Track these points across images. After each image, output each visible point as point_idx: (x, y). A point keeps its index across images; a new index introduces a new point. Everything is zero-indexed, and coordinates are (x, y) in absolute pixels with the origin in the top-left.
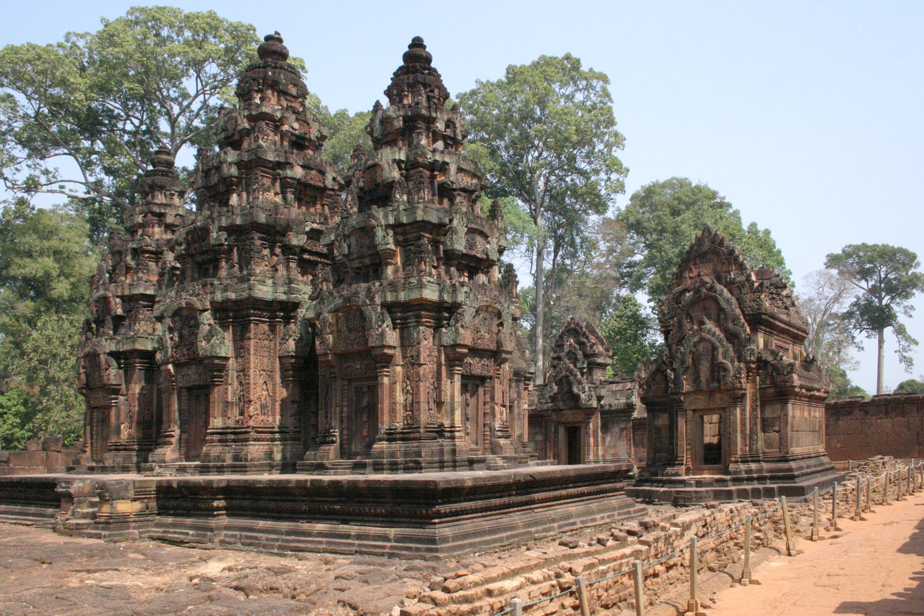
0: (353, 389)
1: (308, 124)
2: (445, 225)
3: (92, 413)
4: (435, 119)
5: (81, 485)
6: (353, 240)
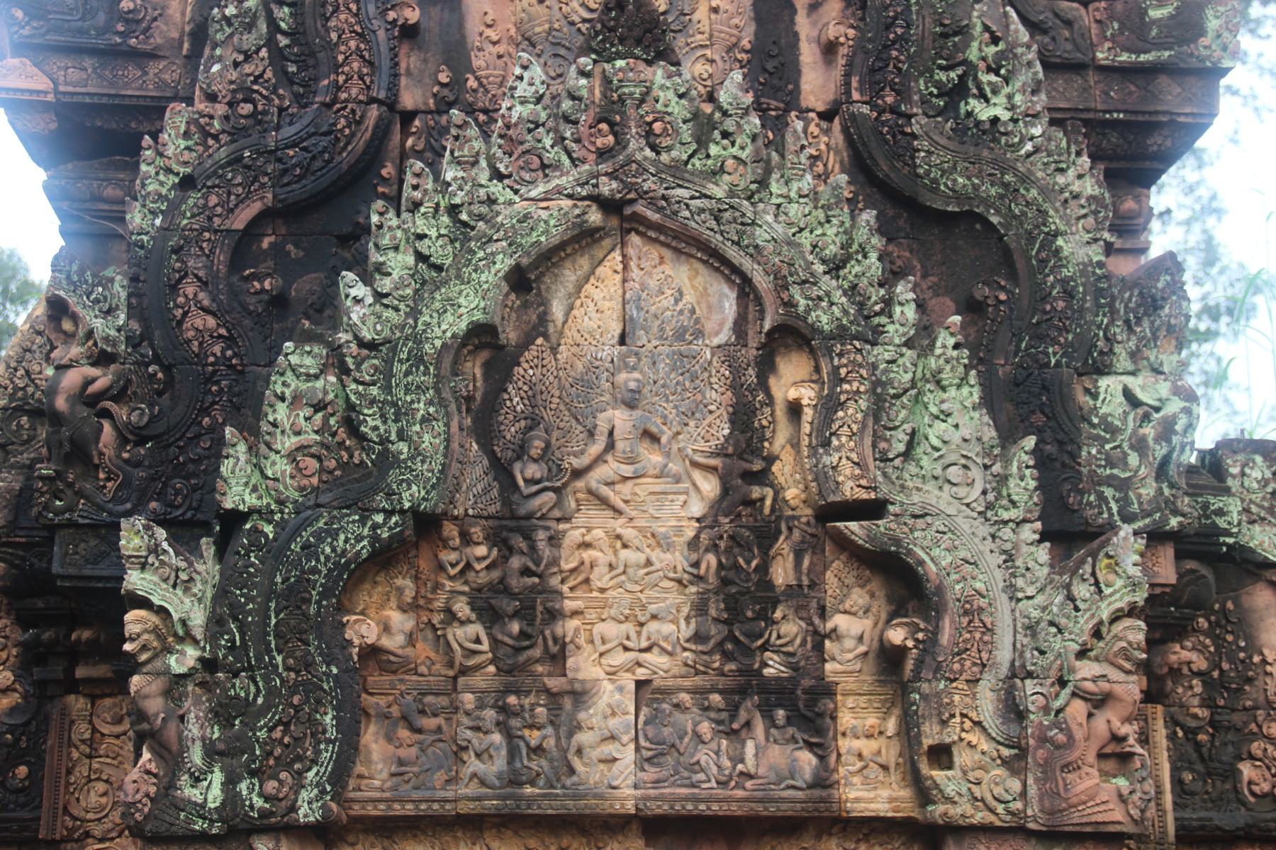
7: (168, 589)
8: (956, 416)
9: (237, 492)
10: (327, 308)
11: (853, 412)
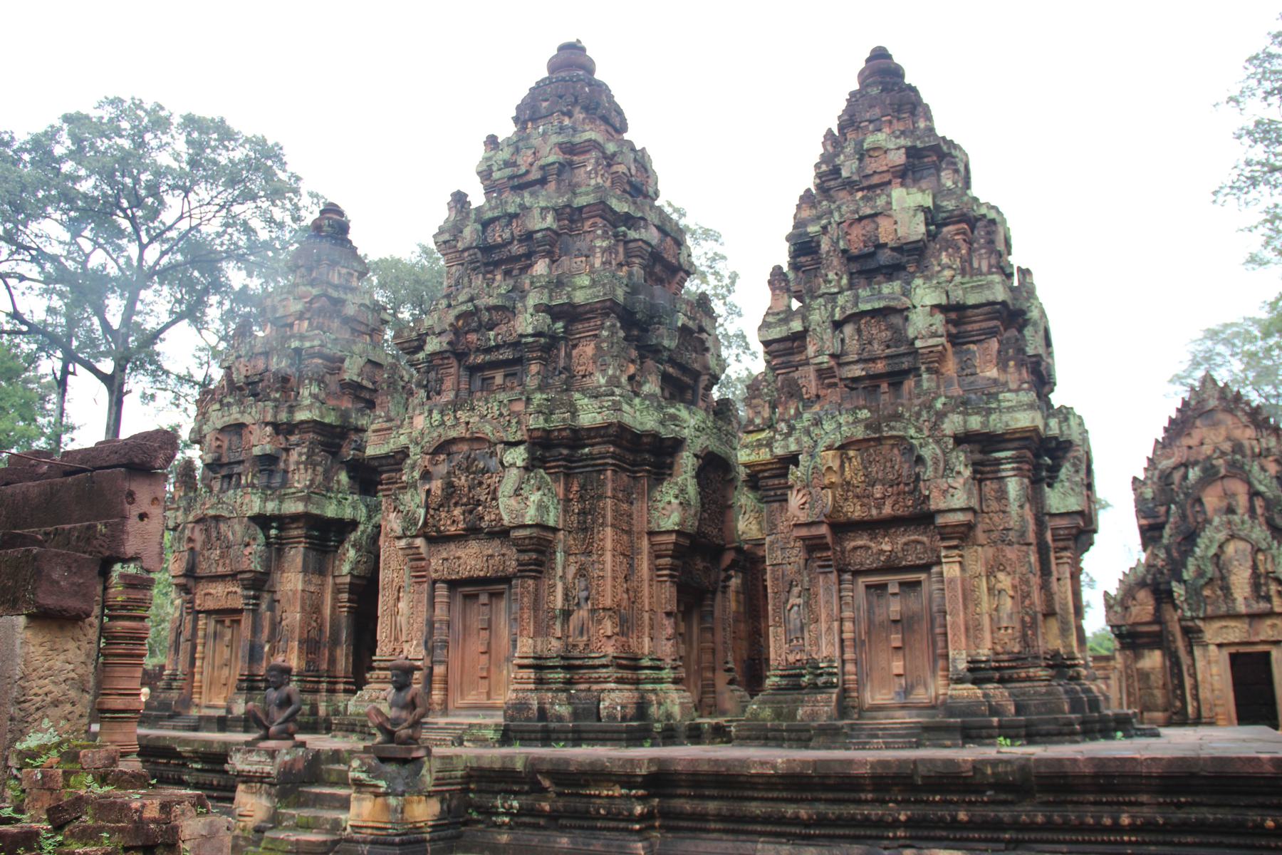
3: (196, 621)
6: (849, 330)
7: (1178, 590)
9: (1186, 576)
10: (1193, 552)
11: (1269, 560)
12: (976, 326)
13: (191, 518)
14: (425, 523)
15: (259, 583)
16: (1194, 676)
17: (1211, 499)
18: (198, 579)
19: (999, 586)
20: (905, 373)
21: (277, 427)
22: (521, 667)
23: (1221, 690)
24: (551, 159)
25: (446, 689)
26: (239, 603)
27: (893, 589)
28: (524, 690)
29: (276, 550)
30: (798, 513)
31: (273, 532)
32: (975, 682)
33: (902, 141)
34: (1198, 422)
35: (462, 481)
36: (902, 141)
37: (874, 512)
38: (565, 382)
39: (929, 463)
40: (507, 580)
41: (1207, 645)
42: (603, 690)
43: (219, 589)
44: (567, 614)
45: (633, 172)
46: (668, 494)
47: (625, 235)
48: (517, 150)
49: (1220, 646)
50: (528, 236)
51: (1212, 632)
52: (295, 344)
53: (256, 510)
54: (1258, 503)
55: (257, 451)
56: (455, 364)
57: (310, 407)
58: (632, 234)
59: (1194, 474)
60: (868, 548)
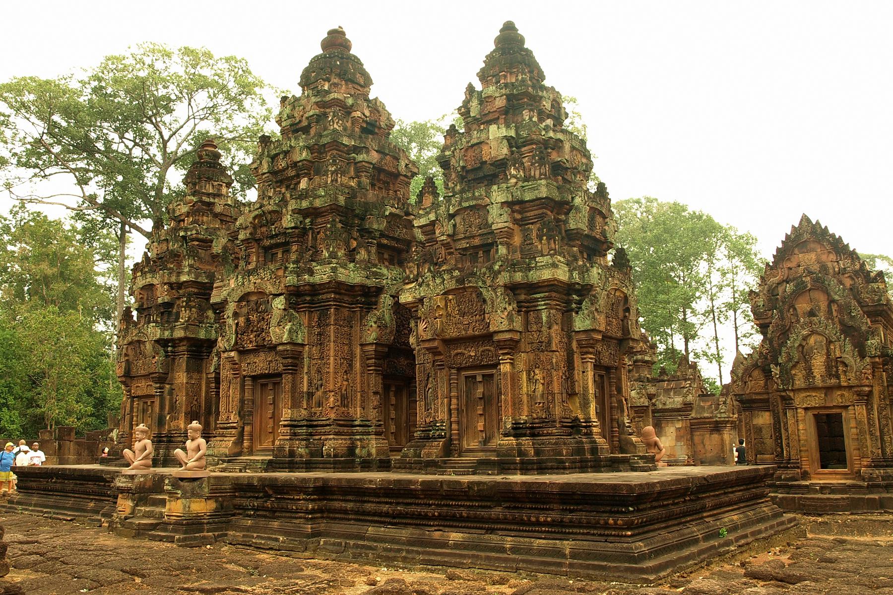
0: (463, 379)
1: (379, 112)
2: (567, 203)
3: (132, 402)
4: (541, 97)
5: (142, 479)
6: (458, 219)
7: (775, 370)
8: (849, 347)
9: (780, 361)
12: (532, 213)
13: (125, 342)
14: (236, 343)
15: (162, 379)
16: (786, 430)
17: (803, 306)
18: (132, 378)
19: (536, 377)
20: (492, 245)
21: (171, 285)
22: (285, 426)
23: (806, 440)
24: (311, 113)
25: (252, 440)
26: (153, 391)
27: (479, 379)
28: (284, 440)
29: (171, 360)
30: (422, 334)
31: (169, 349)
32: (517, 436)
33: (503, 91)
34: (796, 251)
35: (254, 318)
36: (503, 91)
37: (464, 332)
38: (311, 256)
39: (489, 302)
40: (279, 375)
41: (796, 409)
42: (326, 439)
43: (143, 384)
44: (310, 395)
45: (368, 114)
46: (371, 321)
47: (354, 159)
48: (294, 107)
49: (806, 409)
50: (295, 164)
51: (799, 400)
52: (182, 234)
53: (158, 336)
54: (834, 307)
55: (160, 301)
56: (256, 245)
57: (189, 273)
58: (361, 157)
59: (789, 287)
60: (463, 354)
